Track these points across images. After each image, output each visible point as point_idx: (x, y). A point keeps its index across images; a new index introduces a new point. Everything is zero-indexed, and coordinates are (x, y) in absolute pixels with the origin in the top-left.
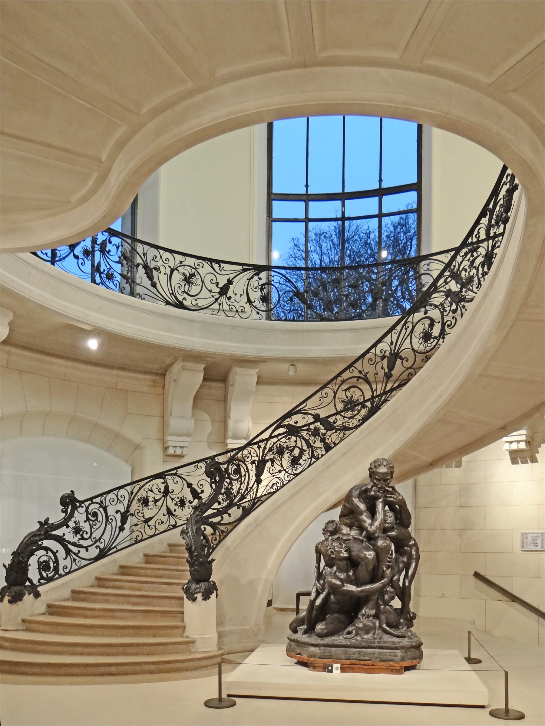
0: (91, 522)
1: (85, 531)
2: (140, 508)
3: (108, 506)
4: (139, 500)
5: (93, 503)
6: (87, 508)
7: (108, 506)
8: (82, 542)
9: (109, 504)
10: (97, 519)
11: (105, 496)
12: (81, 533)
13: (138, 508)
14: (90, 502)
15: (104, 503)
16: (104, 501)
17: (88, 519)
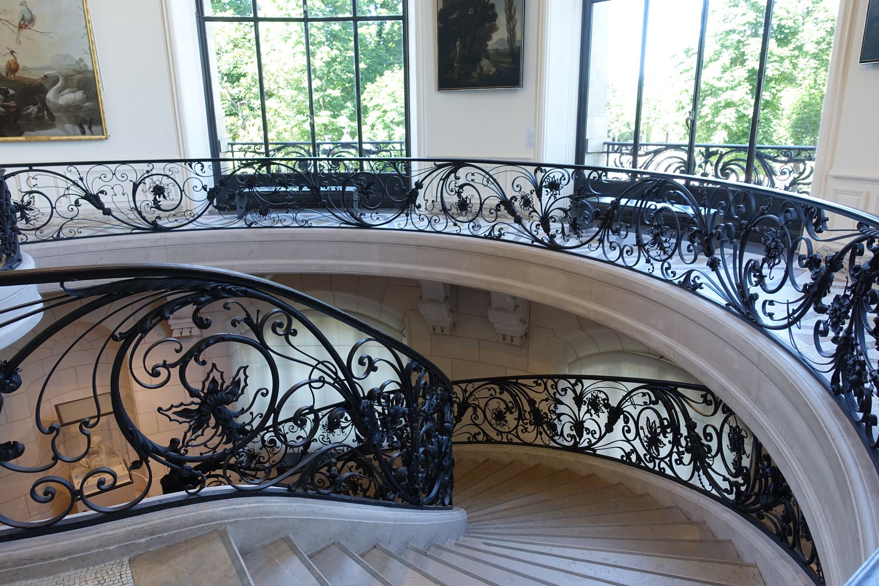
0: (268, 449)
1: (261, 457)
2: (325, 434)
3: (287, 433)
4: (323, 426)
5: (268, 432)
6: (263, 438)
7: (287, 433)
8: (258, 466)
9: (289, 431)
10: (275, 445)
11: (283, 424)
12: (257, 459)
13: (323, 434)
14: (266, 431)
15: (282, 431)
16: (282, 429)
17: (264, 446)
